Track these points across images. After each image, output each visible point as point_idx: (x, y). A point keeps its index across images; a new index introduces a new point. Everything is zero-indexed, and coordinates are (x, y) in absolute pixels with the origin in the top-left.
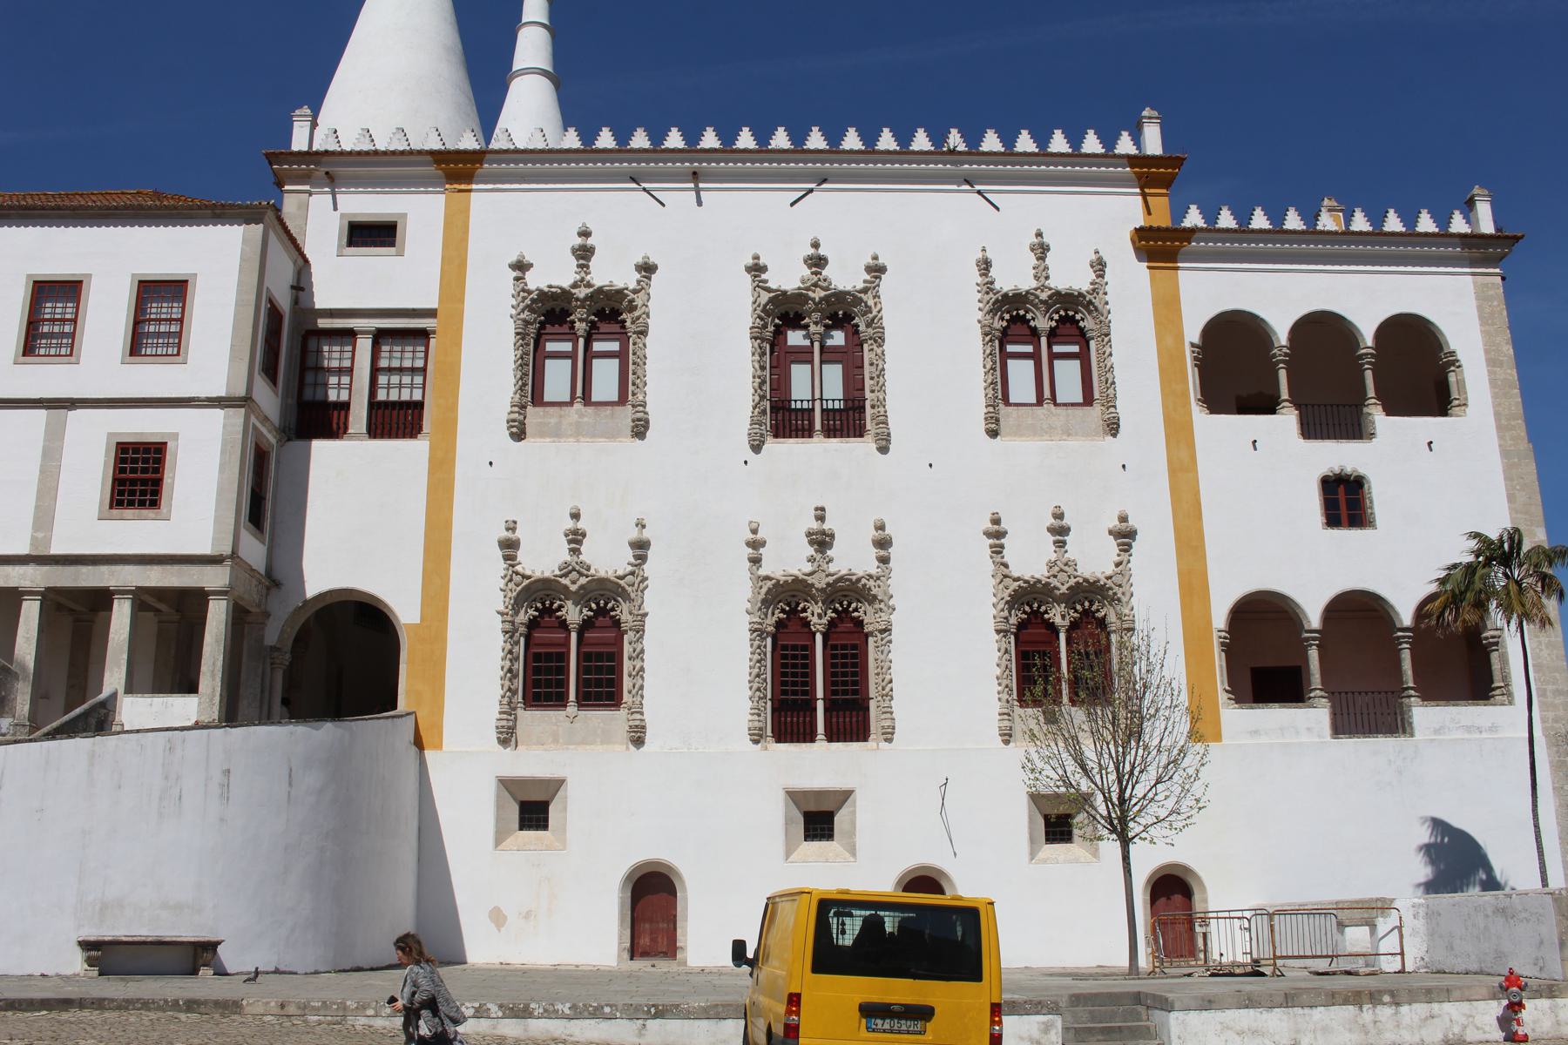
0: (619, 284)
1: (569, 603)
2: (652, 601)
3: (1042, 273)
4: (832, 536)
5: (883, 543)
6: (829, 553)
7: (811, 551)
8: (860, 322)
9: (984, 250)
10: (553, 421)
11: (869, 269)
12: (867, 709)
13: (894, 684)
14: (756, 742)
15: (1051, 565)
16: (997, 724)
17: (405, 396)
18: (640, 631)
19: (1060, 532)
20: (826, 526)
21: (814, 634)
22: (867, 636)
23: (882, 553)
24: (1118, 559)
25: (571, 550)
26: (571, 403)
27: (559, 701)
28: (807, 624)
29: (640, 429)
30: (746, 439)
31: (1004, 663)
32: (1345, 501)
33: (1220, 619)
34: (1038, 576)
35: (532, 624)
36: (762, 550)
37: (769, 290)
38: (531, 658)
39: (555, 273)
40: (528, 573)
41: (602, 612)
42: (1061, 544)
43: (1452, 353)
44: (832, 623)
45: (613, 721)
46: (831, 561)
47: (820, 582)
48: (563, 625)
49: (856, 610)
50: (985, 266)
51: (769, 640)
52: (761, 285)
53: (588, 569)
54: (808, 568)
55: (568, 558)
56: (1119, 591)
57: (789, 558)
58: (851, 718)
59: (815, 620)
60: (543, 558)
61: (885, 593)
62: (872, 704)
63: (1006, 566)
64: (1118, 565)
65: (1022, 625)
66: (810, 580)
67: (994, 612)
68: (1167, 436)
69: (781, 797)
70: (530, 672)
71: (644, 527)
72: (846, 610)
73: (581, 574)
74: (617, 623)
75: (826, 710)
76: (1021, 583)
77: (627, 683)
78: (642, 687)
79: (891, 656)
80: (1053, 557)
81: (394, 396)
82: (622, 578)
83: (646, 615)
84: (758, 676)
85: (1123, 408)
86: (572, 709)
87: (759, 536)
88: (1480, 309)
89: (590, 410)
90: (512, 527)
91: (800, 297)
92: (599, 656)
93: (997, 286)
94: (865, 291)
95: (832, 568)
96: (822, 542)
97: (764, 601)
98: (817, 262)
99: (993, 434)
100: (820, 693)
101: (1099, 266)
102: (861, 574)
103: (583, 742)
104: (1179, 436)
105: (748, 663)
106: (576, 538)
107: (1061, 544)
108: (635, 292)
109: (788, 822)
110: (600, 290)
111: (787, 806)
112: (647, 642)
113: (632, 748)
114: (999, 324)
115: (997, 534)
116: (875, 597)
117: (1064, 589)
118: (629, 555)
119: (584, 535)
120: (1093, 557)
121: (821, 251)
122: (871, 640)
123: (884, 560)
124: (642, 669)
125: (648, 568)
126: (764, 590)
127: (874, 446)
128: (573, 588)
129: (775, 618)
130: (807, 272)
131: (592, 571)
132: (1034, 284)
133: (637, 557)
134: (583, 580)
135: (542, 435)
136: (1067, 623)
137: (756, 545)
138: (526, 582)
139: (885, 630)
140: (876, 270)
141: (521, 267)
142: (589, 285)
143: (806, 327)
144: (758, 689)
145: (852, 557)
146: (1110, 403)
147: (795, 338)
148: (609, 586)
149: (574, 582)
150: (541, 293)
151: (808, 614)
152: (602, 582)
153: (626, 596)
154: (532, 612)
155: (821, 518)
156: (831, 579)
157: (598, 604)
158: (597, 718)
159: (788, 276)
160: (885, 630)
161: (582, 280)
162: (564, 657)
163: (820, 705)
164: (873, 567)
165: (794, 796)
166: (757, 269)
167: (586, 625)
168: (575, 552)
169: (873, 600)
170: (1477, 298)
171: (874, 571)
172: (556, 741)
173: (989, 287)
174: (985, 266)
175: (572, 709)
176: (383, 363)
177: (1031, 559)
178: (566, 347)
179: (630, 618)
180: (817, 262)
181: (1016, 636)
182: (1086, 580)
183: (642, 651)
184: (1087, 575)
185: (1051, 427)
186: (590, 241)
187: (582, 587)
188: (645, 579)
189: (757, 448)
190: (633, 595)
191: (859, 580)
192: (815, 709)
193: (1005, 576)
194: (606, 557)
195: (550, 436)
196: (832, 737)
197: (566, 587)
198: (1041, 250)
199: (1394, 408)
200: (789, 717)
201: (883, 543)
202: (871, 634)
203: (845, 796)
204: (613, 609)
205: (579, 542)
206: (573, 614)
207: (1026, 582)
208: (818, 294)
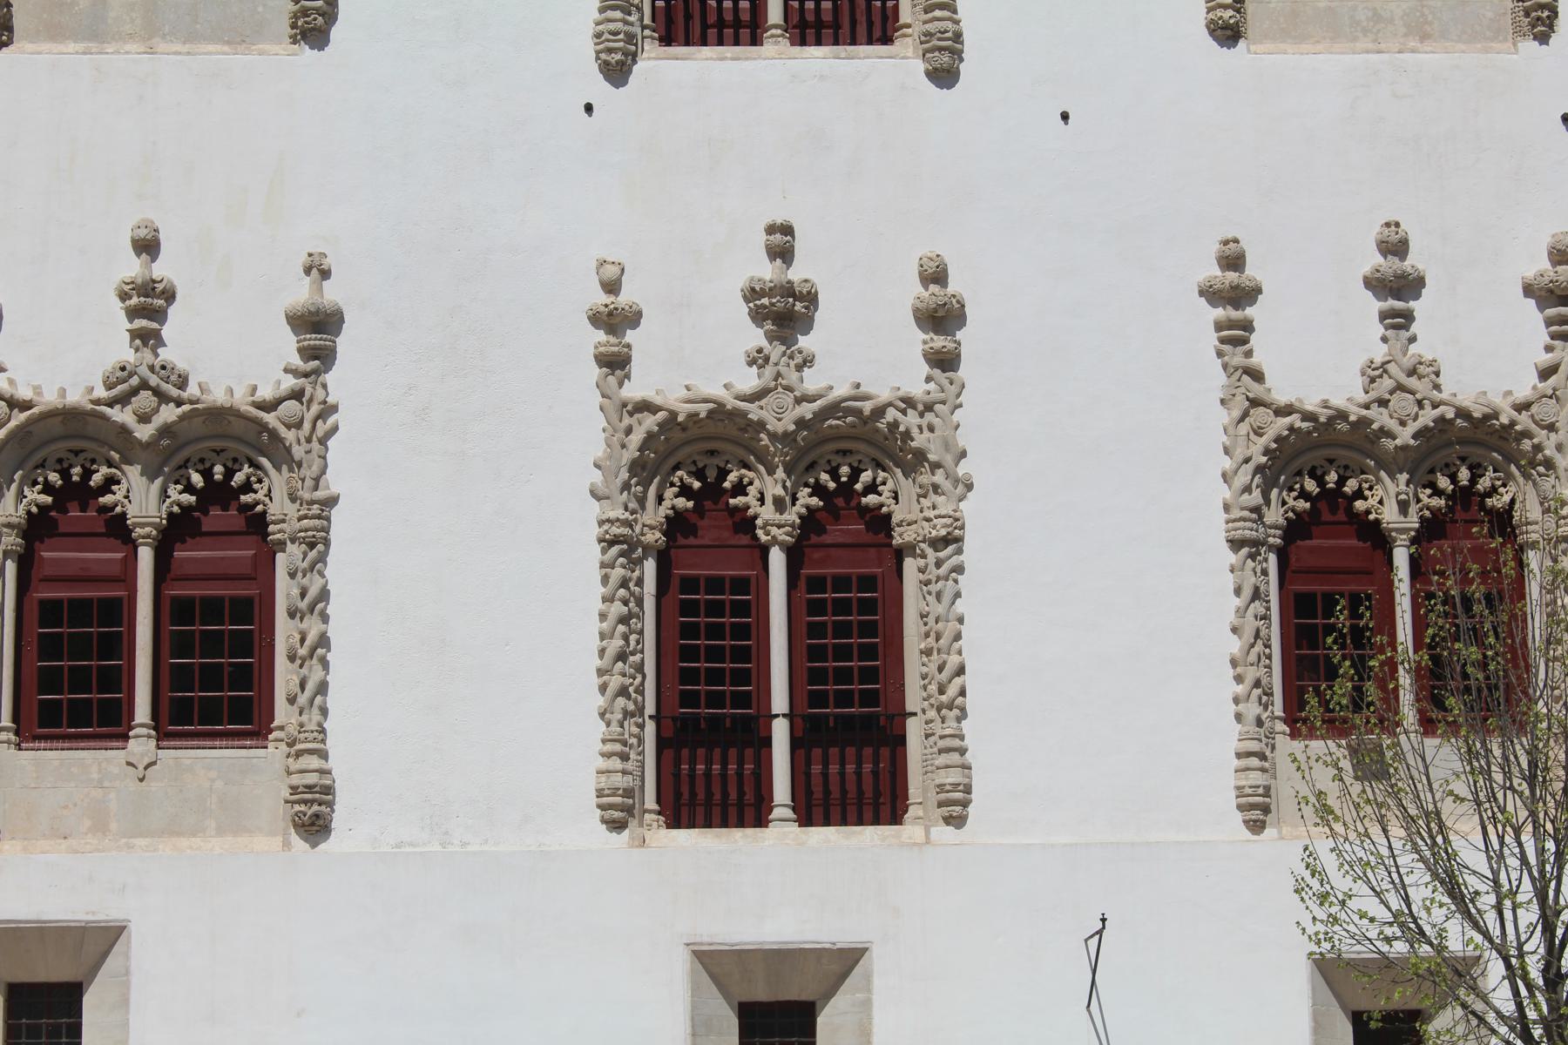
1: (133, 473)
2: (344, 469)
4: (811, 299)
5: (941, 318)
7: (756, 337)
12: (901, 740)
13: (968, 679)
14: (617, 826)
15: (1374, 373)
16: (1231, 781)
18: (317, 542)
19: (1397, 289)
20: (796, 274)
22: (899, 554)
23: (940, 342)
24: (1545, 359)
25: (135, 334)
27: (109, 723)
28: (745, 523)
30: (589, 49)
31: (1250, 624)
34: (1339, 401)
36: (630, 336)
38: (33, 614)
40: (24, 393)
41: (218, 494)
42: (1398, 321)
44: (810, 521)
45: (249, 774)
46: (808, 362)
47: (779, 416)
48: (118, 528)
49: (872, 488)
51: (650, 566)
53: (182, 383)
54: (749, 380)
55: (129, 356)
56: (1549, 442)
57: (701, 357)
58: (860, 764)
59: (767, 513)
61: (947, 446)
62: (914, 728)
63: (1257, 376)
64: (1546, 373)
65: (1295, 529)
66: (754, 412)
67: (1227, 494)
69: (680, 966)
70: (31, 649)
71: (325, 274)
72: (846, 490)
73: (162, 397)
74: (257, 523)
75: (795, 744)
76: (1295, 420)
77: (284, 676)
78: (322, 688)
79: (960, 606)
80: (1380, 353)
82: (270, 406)
83: (332, 501)
84: (622, 656)
86: (141, 745)
87: (624, 299)
92: (212, 610)
95: (812, 381)
96: (784, 312)
97: (636, 467)
99: (1228, 34)
100: (780, 700)
102: (884, 395)
103: (172, 829)
105: (595, 626)
106: (148, 305)
107: (1398, 321)
111: (695, 989)
112: (339, 571)
113: (298, 843)
115: (1233, 294)
116: (920, 455)
117: (1405, 436)
118: (287, 346)
119: (170, 296)
122: (910, 565)
124: (324, 641)
125: (338, 382)
126: (637, 438)
127: (920, 67)
128: (144, 433)
129: (664, 510)
131: (192, 390)
133: (308, 353)
134: (169, 414)
135: (54, 33)
136: (1413, 522)
137: (615, 321)
138: (19, 418)
139: (946, 541)
144: (623, 692)
145: (862, 353)
148: (238, 427)
149: (144, 418)
152: (219, 415)
153: (283, 456)
154: (35, 496)
155: (782, 254)
156: (807, 410)
157: (207, 474)
158: (207, 766)
160: (946, 541)
162: (118, 612)
163: (780, 732)
164: (915, 379)
165: (714, 963)
167: (178, 528)
168: (147, 339)
169: (913, 462)
172: (100, 827)
175: (141, 745)
177: (1321, 359)
179: (292, 510)
181: (1282, 554)
182: (1463, 413)
183: (324, 595)
184: (1466, 400)
185: (1377, 17)
187: (166, 431)
188: (329, 410)
189: (617, 72)
190: (298, 452)
191: (879, 412)
192: (767, 742)
193: (1255, 403)
194: (229, 354)
195: (76, 37)
196: (810, 811)
197: (124, 430)
200: (699, 763)
201: (941, 318)
202: (910, 549)
203: (844, 963)
204: (247, 487)
205: (159, 315)
206: (143, 500)
207: (1308, 416)
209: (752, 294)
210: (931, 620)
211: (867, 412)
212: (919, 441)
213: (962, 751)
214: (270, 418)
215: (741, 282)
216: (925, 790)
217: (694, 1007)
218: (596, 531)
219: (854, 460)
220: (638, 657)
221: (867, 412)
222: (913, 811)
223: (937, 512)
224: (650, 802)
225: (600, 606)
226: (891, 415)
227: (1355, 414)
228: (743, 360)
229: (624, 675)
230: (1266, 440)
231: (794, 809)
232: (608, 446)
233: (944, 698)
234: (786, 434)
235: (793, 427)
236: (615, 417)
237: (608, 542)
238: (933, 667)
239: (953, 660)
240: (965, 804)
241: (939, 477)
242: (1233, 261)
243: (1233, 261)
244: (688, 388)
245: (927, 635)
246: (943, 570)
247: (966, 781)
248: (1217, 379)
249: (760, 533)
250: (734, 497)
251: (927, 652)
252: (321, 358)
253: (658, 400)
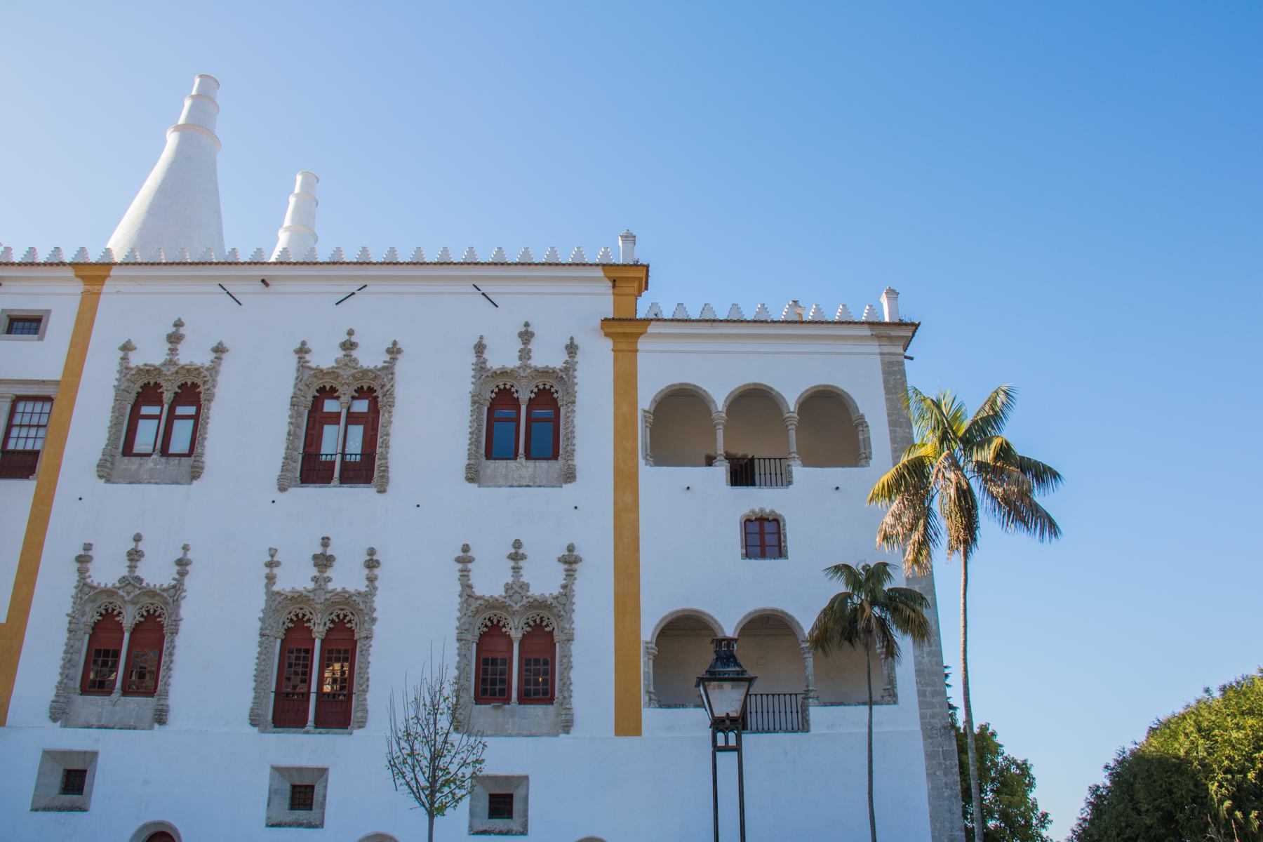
0: (198, 363)
3: (525, 354)
5: (372, 564)
6: (329, 573)
7: (314, 572)
8: (379, 393)
9: (481, 337)
10: (134, 467)
11: (389, 351)
15: (508, 587)
17: (29, 447)
20: (329, 552)
26: (149, 455)
28: (309, 630)
29: (195, 474)
32: (763, 537)
33: (648, 631)
34: (496, 595)
35: (96, 627)
36: (276, 571)
37: (310, 368)
39: (151, 354)
40: (95, 584)
42: (516, 569)
43: (862, 417)
46: (329, 580)
49: (350, 621)
50: (480, 348)
52: (302, 366)
54: (311, 586)
55: (126, 574)
57: (297, 577)
59: (315, 629)
60: (107, 573)
63: (470, 587)
68: (616, 484)
80: (510, 580)
81: (20, 447)
85: (582, 460)
87: (276, 559)
88: (886, 381)
89: (163, 460)
90: (88, 547)
91: (332, 373)
93: (489, 365)
94: (384, 368)
95: (330, 586)
98: (348, 346)
101: (572, 349)
104: (626, 481)
106: (135, 556)
107: (516, 569)
108: (208, 369)
109: (273, 793)
110: (183, 368)
111: (272, 779)
114: (489, 396)
115: (465, 558)
120: (543, 581)
121: (354, 339)
123: (371, 580)
125: (188, 581)
130: (340, 353)
131: (144, 585)
132: (518, 363)
136: (520, 635)
139: (367, 638)
140: (394, 351)
141: (127, 347)
142: (175, 364)
143: (338, 398)
146: (570, 454)
147: (330, 406)
150: (139, 370)
151: (311, 624)
152: (152, 593)
156: (328, 596)
159: (325, 357)
160: (367, 638)
161: (171, 361)
162: (117, 654)
164: (362, 587)
166: (302, 350)
167: (136, 629)
170: (884, 372)
171: (363, 589)
173: (480, 367)
174: (480, 348)
176: (17, 420)
178: (155, 410)
180: (348, 346)
186: (182, 330)
189: (282, 489)
191: (351, 596)
193: (469, 596)
194: (156, 574)
198: (526, 336)
199: (810, 460)
201: (372, 564)
203: (322, 772)
206: (129, 618)
208: (346, 374)
212: (362, 606)
214: (165, 594)
217: (271, 785)
224: (270, 717)
227: (501, 599)
230: (473, 608)
242: (466, 549)
243: (466, 549)
248: (459, 588)
252: (182, 574)
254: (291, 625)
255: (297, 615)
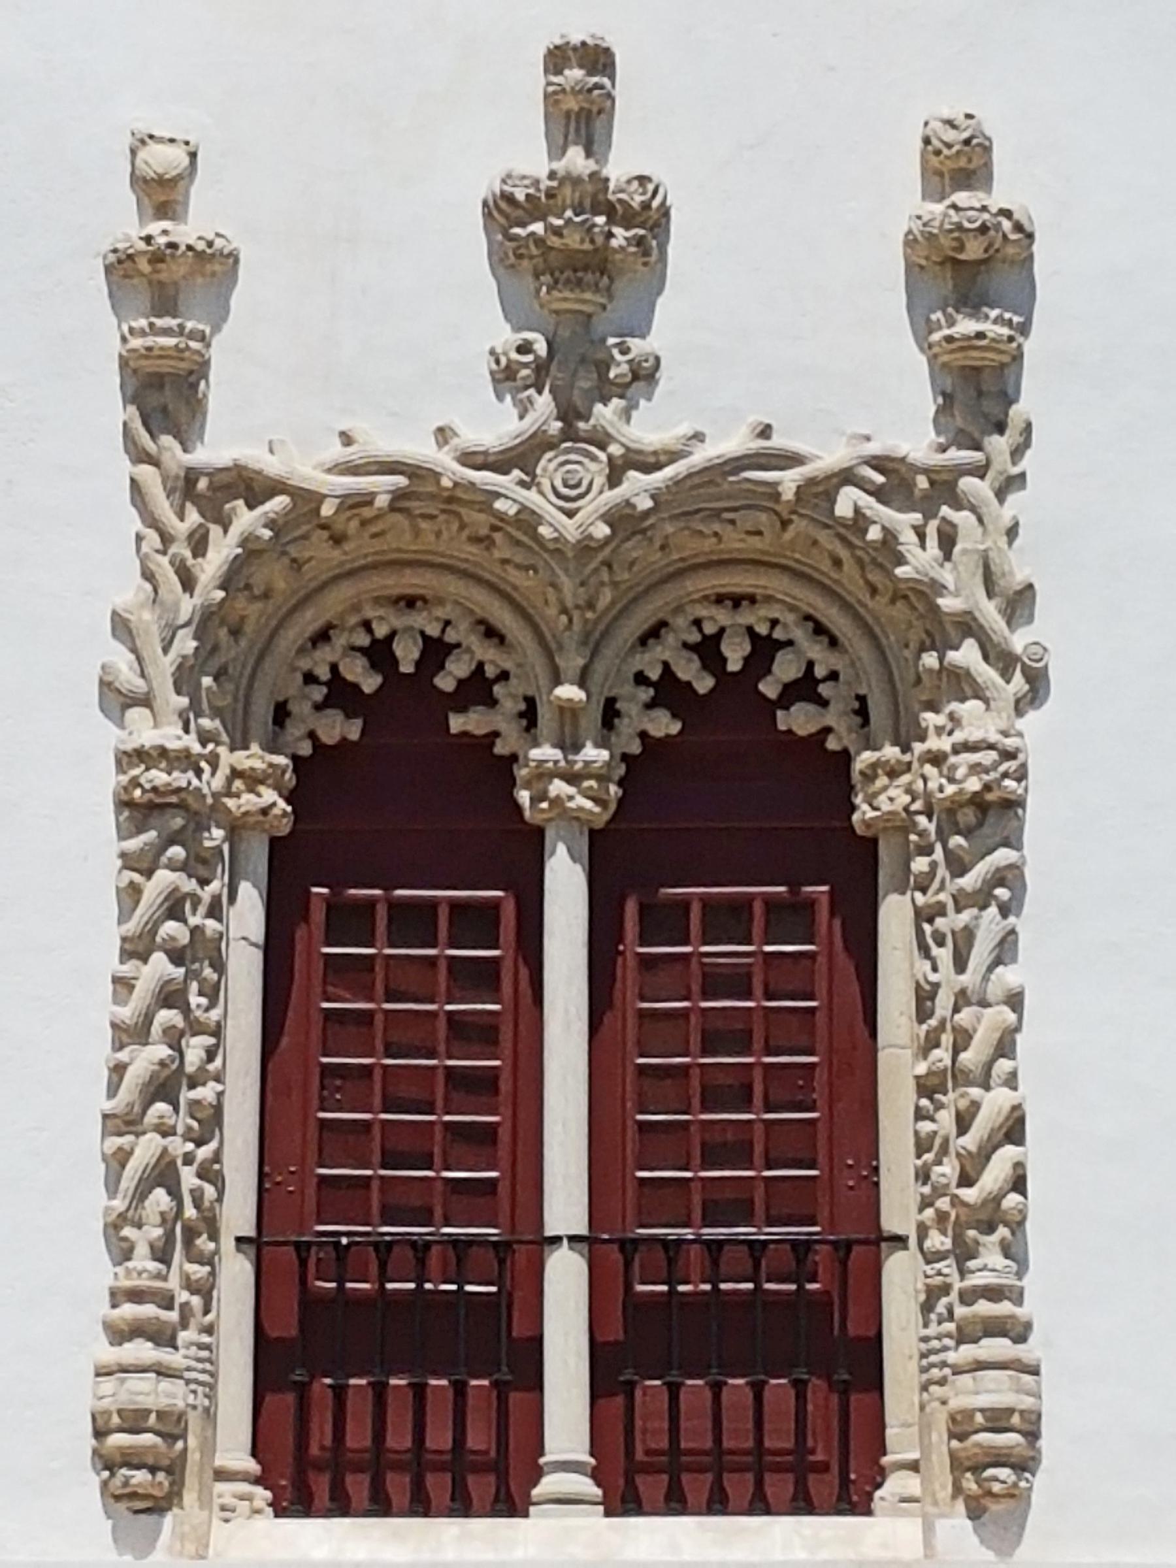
4: (650, 221)
13: (1036, 1151)
21: (533, 845)
47: (571, 507)
49: (804, 688)
84: (163, 1086)
100: (565, 1205)
102: (830, 456)
105: (101, 1011)
144: (163, 1174)
156: (638, 488)
171: (916, 438)
196: (632, 1481)
209: (504, 211)
210: (943, 1003)
211: (788, 492)
212: (920, 560)
213: (1020, 1333)
215: (486, 185)
216: (925, 1428)
218: (110, 780)
219: (757, 619)
220: (206, 1093)
221: (788, 492)
222: (896, 1485)
223: (959, 736)
225: (113, 964)
226: (847, 501)
228: (484, 366)
229: (166, 1132)
231: (596, 1475)
232: (148, 576)
233: (970, 1195)
234: (587, 547)
235: (602, 530)
236: (164, 508)
237: (137, 810)
238: (946, 1120)
239: (994, 1103)
240: (1025, 1465)
241: (967, 655)
244: (347, 439)
245: (931, 1042)
246: (969, 881)
247: (1027, 1402)
249: (524, 796)
250: (462, 709)
251: (929, 1087)
253: (272, 466)
254: (338, 728)
255: (380, 654)
